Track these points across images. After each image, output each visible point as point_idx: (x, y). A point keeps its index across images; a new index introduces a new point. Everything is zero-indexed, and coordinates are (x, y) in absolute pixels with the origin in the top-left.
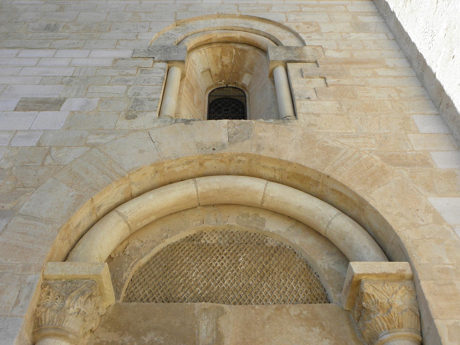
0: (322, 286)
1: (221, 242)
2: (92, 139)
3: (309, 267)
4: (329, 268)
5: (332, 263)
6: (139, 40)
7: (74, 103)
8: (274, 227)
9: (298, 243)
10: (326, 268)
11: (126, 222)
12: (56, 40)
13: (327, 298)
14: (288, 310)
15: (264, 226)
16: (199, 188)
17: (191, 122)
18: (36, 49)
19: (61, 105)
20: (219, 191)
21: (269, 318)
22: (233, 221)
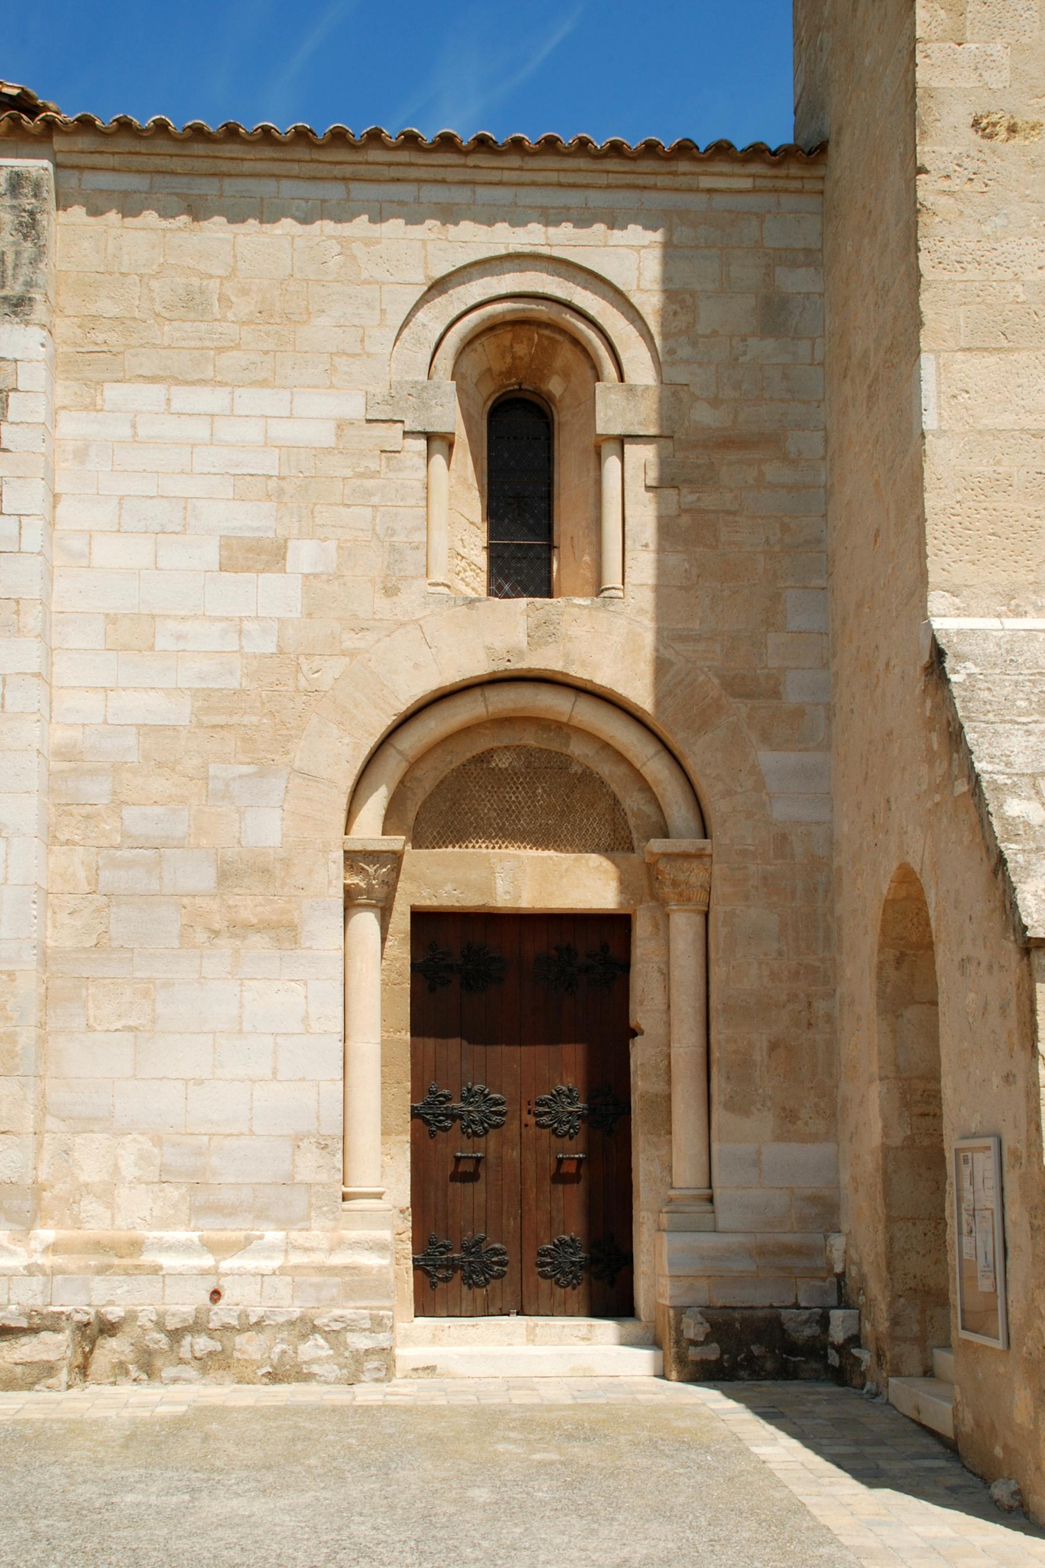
0: (628, 827)
1: (515, 763)
2: (351, 641)
3: (616, 801)
4: (639, 809)
5: (643, 802)
6: (369, 355)
7: (304, 555)
8: (578, 749)
9: (607, 773)
10: (635, 809)
11: (407, 761)
12: (220, 350)
13: (631, 843)
14: (587, 861)
15: (568, 747)
16: (490, 709)
17: (477, 604)
18: (193, 383)
19: (284, 559)
20: (514, 710)
21: (567, 870)
22: (530, 739)
